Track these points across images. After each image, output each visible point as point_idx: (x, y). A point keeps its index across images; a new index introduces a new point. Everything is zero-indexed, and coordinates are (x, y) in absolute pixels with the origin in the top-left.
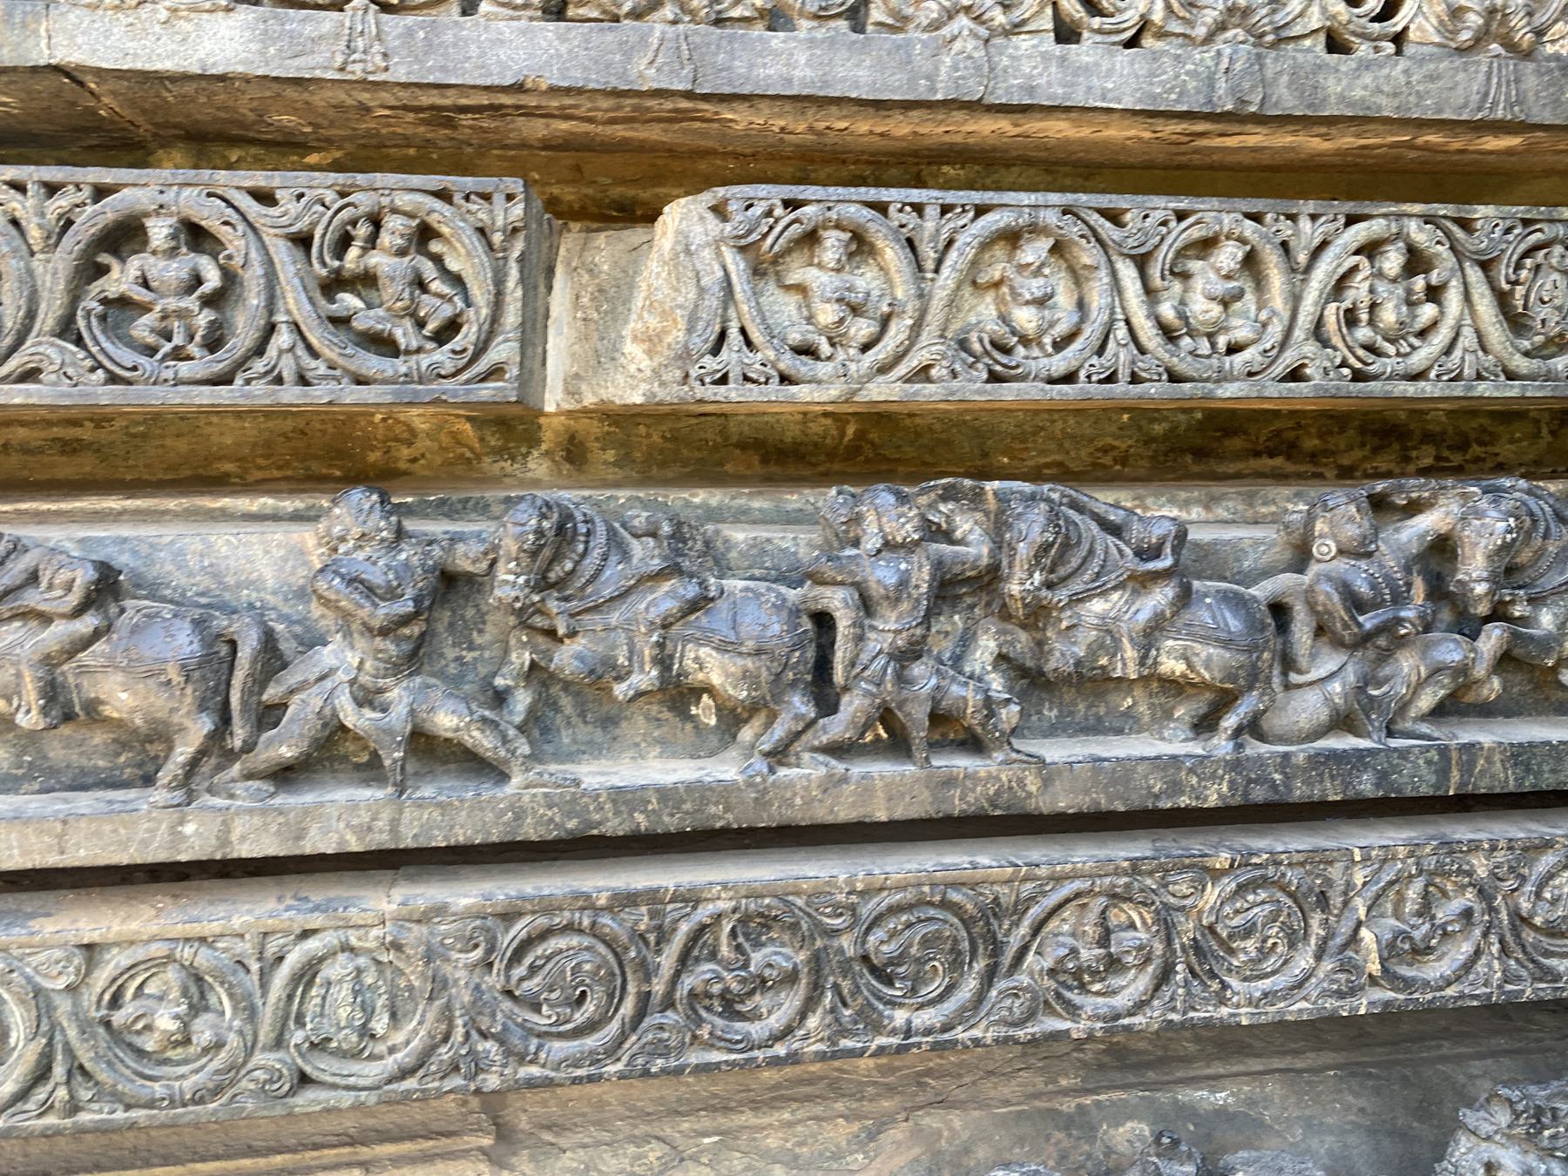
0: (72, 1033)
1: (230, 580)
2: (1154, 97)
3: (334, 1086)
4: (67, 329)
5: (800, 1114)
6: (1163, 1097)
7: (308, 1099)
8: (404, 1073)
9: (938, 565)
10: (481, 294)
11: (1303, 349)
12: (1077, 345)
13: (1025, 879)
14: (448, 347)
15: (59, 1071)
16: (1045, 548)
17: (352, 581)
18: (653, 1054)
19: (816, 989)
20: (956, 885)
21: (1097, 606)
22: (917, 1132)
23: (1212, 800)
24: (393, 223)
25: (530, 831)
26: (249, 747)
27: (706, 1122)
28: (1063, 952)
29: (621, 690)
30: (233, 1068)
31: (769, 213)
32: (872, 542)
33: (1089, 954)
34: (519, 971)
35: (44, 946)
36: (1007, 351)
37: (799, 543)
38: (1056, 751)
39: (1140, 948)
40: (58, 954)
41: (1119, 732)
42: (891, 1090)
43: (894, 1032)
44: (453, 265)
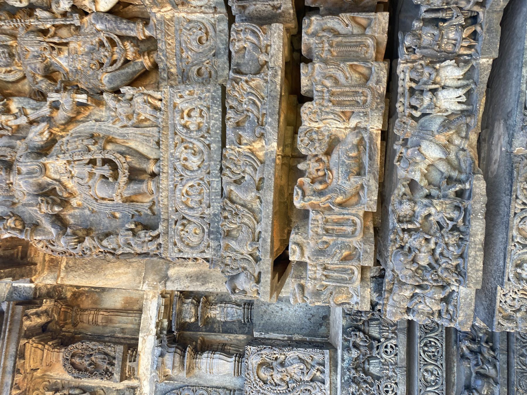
11: (438, 363)
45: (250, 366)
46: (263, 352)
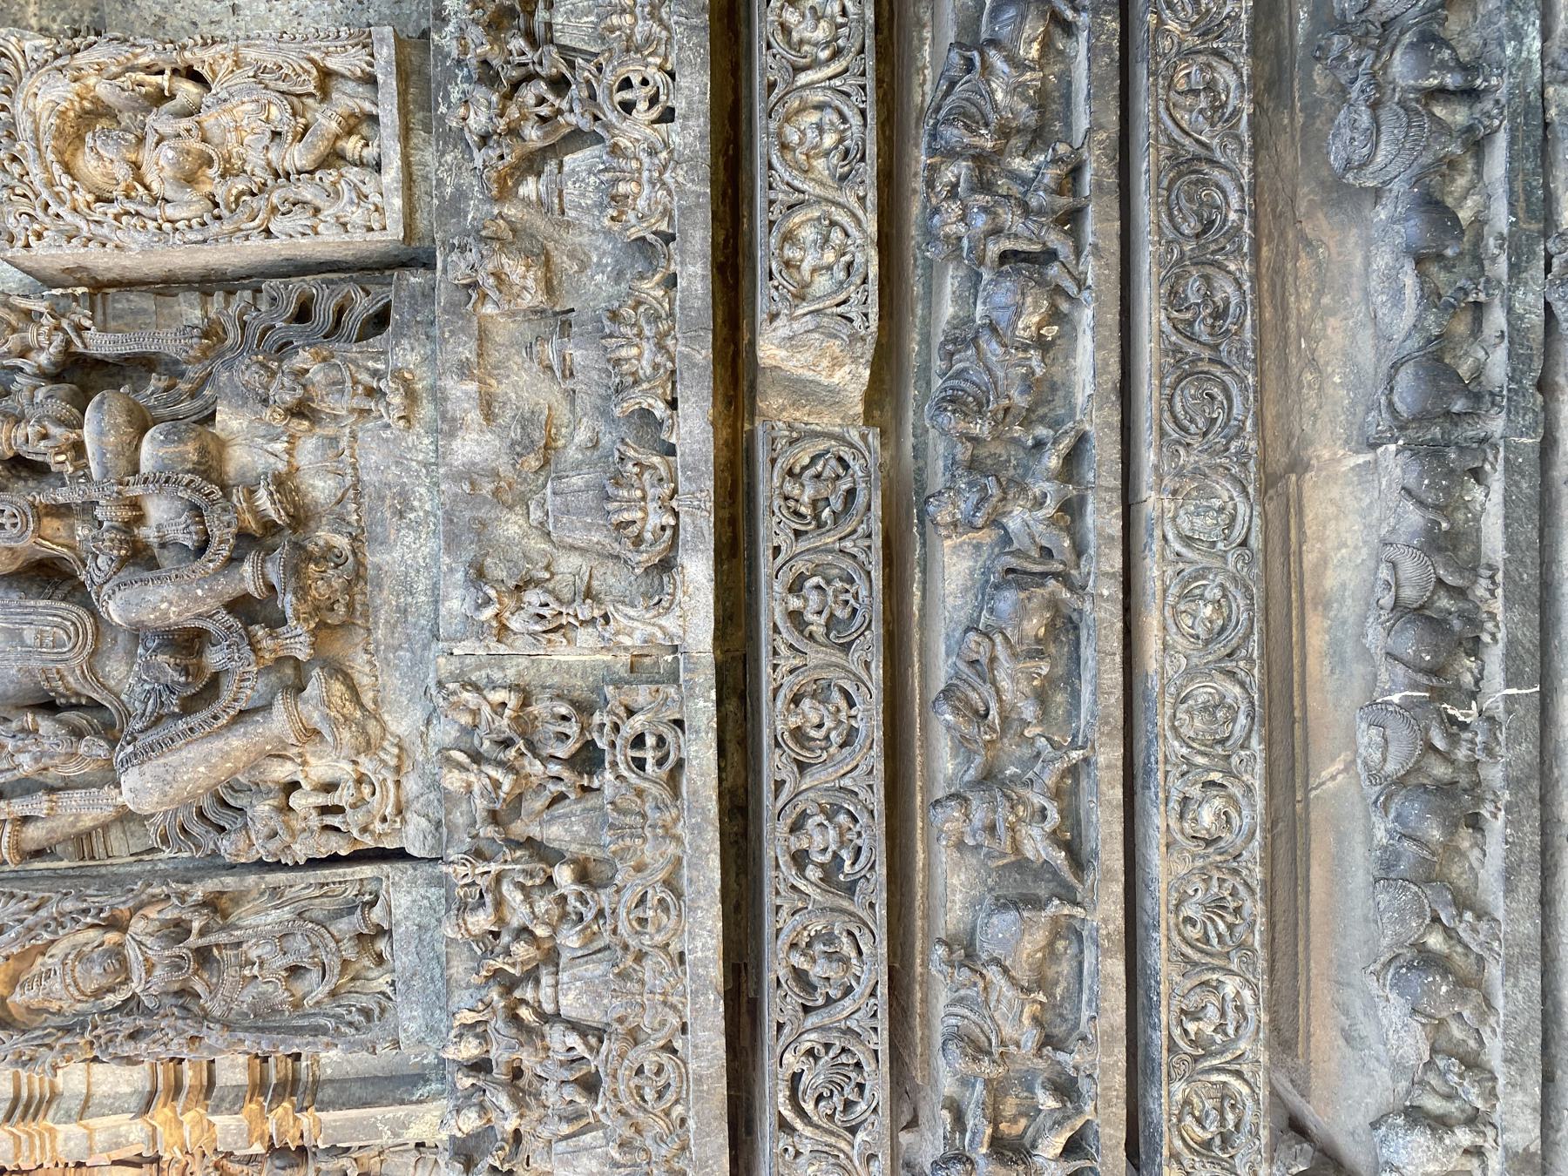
0: (1210, 658)
1: (969, 583)
2: (703, 63)
3: (1249, 529)
4: (846, 648)
5: (1292, 290)
6: (1300, 55)
7: (1255, 542)
8: (1244, 491)
9: (973, 190)
10: (822, 446)
12: (845, 110)
13: (1157, 140)
14: (851, 463)
15: (1230, 665)
16: (966, 126)
17: (977, 508)
18: (1245, 357)
19: (1213, 263)
20: (1158, 183)
21: (999, 96)
22: (1310, 215)
23: (1115, 25)
24: (788, 487)
25: (1116, 419)
26: (1063, 562)
27: (1293, 347)
28: (1201, 118)
29: (1039, 372)
30: (1234, 579)
31: (776, 288)
32: (962, 228)
33: (1203, 103)
34: (1193, 429)
35: (1163, 667)
36: (847, 152)
37: (951, 281)
38: (1082, 122)
39: (1201, 70)
40: (1168, 661)
41: (1070, 83)
42: (1282, 234)
43: (1241, 220)
44: (806, 461)
45: (24, 125)
46: (81, 59)
